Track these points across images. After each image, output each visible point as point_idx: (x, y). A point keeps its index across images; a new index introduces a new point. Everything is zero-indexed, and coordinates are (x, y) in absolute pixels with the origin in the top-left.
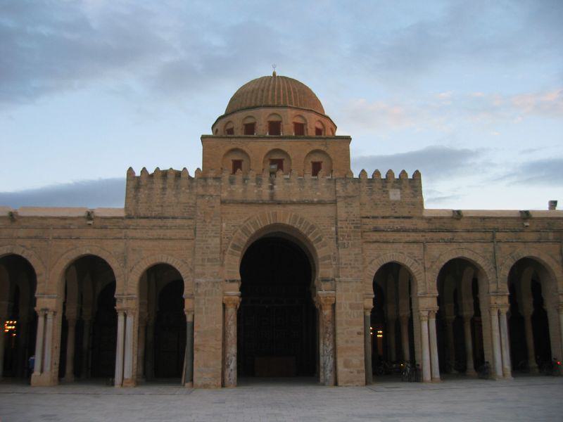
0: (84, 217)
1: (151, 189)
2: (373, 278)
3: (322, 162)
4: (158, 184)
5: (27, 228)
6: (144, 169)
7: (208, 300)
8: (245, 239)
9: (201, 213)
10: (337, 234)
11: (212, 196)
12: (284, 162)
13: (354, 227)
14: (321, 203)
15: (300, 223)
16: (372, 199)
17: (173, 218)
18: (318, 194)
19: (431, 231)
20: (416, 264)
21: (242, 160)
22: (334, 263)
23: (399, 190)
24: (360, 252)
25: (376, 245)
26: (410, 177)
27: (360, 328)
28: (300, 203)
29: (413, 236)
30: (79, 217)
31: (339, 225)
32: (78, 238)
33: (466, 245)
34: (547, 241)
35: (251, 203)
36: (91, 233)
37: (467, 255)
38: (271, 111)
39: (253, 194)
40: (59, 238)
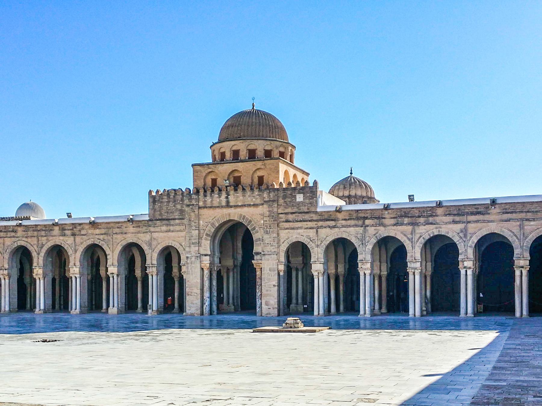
4: (165, 199)
5: (100, 229)
8: (213, 230)
11: (193, 205)
15: (243, 219)
16: (285, 202)
19: (321, 220)
20: (311, 243)
25: (287, 231)
26: (311, 185)
27: (275, 282)
29: (310, 224)
32: (126, 233)
33: (344, 229)
34: (402, 224)
35: (215, 207)
36: (131, 228)
37: (344, 236)
38: (233, 143)
39: (216, 203)
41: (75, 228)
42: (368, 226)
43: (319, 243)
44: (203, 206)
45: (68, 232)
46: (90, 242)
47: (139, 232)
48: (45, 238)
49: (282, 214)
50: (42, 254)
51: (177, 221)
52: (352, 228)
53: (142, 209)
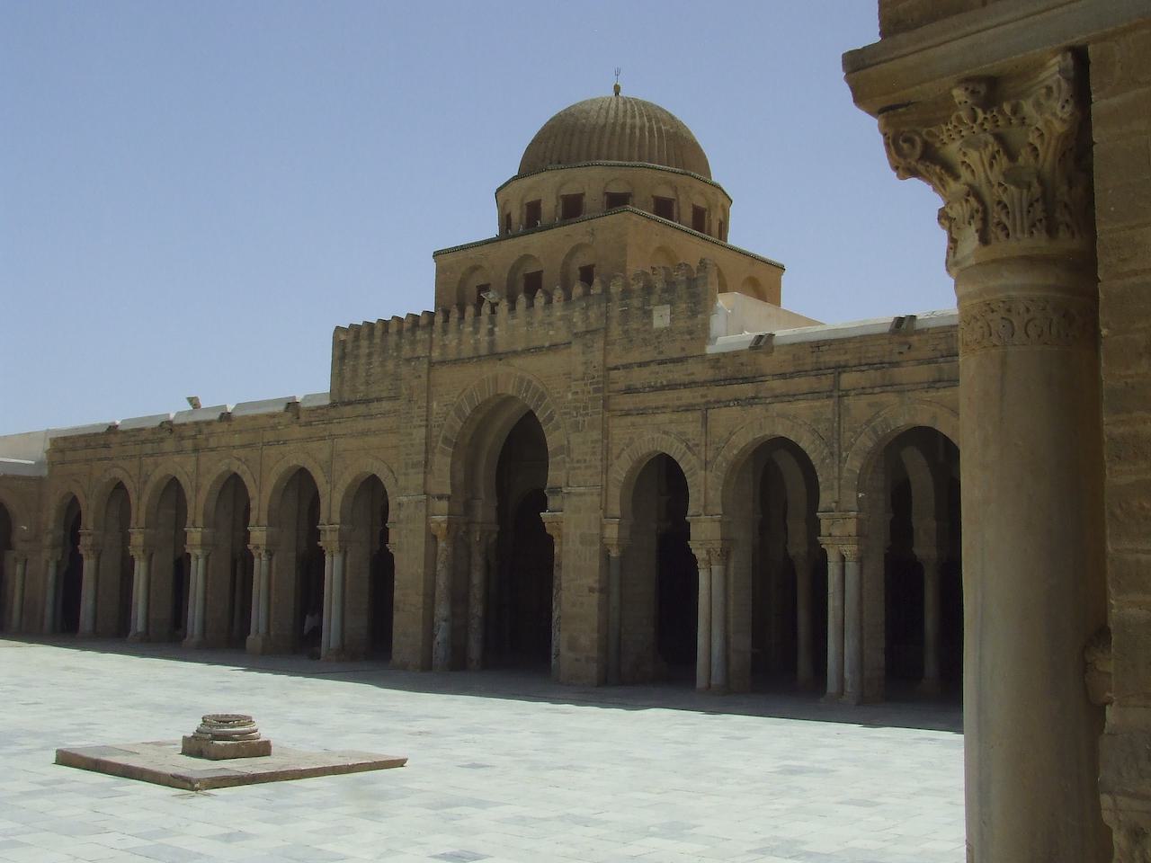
1: (357, 357)
5: (241, 432)
7: (411, 530)
8: (458, 426)
9: (406, 390)
11: (418, 358)
13: (596, 390)
14: (554, 347)
15: (527, 391)
18: (551, 333)
19: (715, 382)
22: (567, 459)
23: (669, 306)
24: (601, 437)
25: (629, 419)
27: (591, 580)
28: (528, 351)
29: (687, 396)
33: (777, 407)
36: (297, 431)
37: (780, 430)
39: (467, 351)
40: (268, 444)
41: (200, 432)
43: (710, 455)
44: (440, 359)
45: (188, 444)
46: (222, 467)
47: (310, 439)
48: (149, 461)
49: (616, 368)
50: (145, 499)
51: (386, 405)
52: (802, 404)
53: (311, 379)
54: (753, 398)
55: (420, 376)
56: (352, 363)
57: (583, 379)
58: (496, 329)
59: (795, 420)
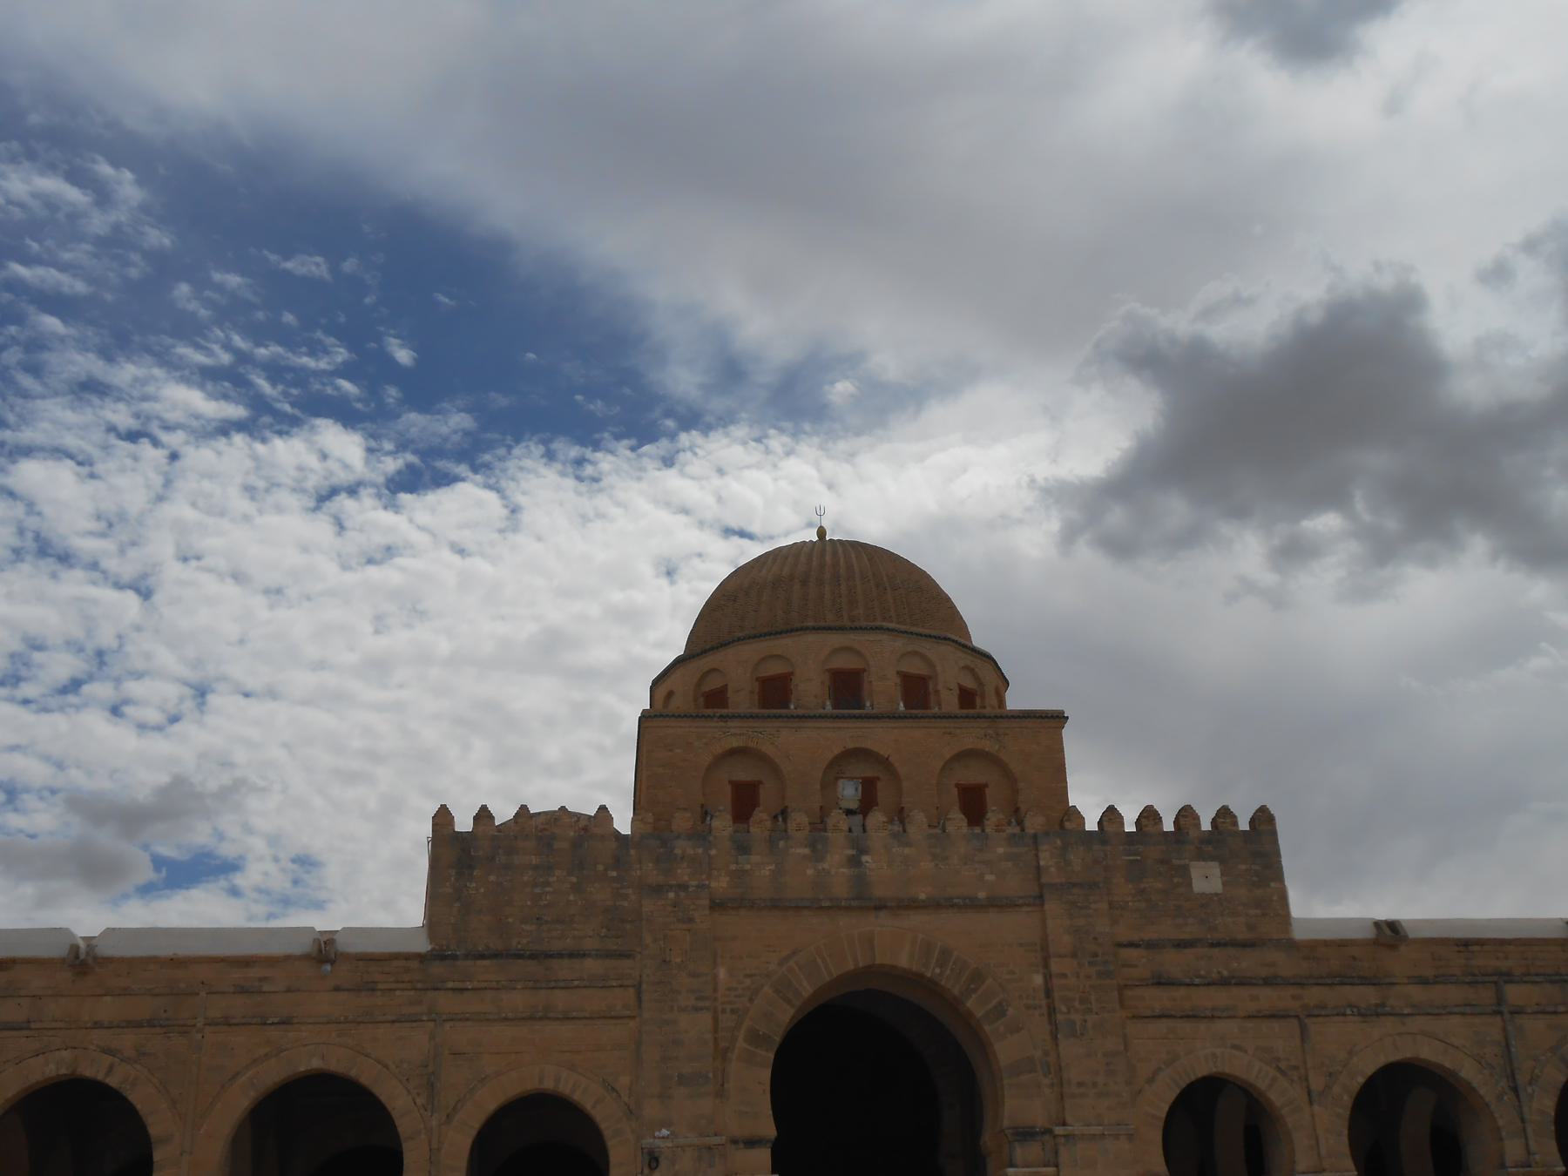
0: (306, 957)
2: (1161, 1124)
3: (986, 785)
6: (484, 809)
8: (785, 1016)
10: (1048, 993)
11: (683, 887)
12: (879, 785)
17: (571, 955)
18: (989, 877)
21: (760, 782)
22: (1046, 1081)
24: (1122, 1048)
29: (1268, 998)
30: (288, 958)
31: (1055, 966)
32: (286, 1022)
37: (1428, 1052)
38: (836, 640)
40: (227, 1022)
42: (1517, 1011)
49: (1131, 945)
51: (592, 966)
52: (1455, 1020)
54: (1383, 1005)
55: (691, 920)
56: (492, 878)
57: (1074, 955)
58: (865, 858)
59: (1453, 1044)
